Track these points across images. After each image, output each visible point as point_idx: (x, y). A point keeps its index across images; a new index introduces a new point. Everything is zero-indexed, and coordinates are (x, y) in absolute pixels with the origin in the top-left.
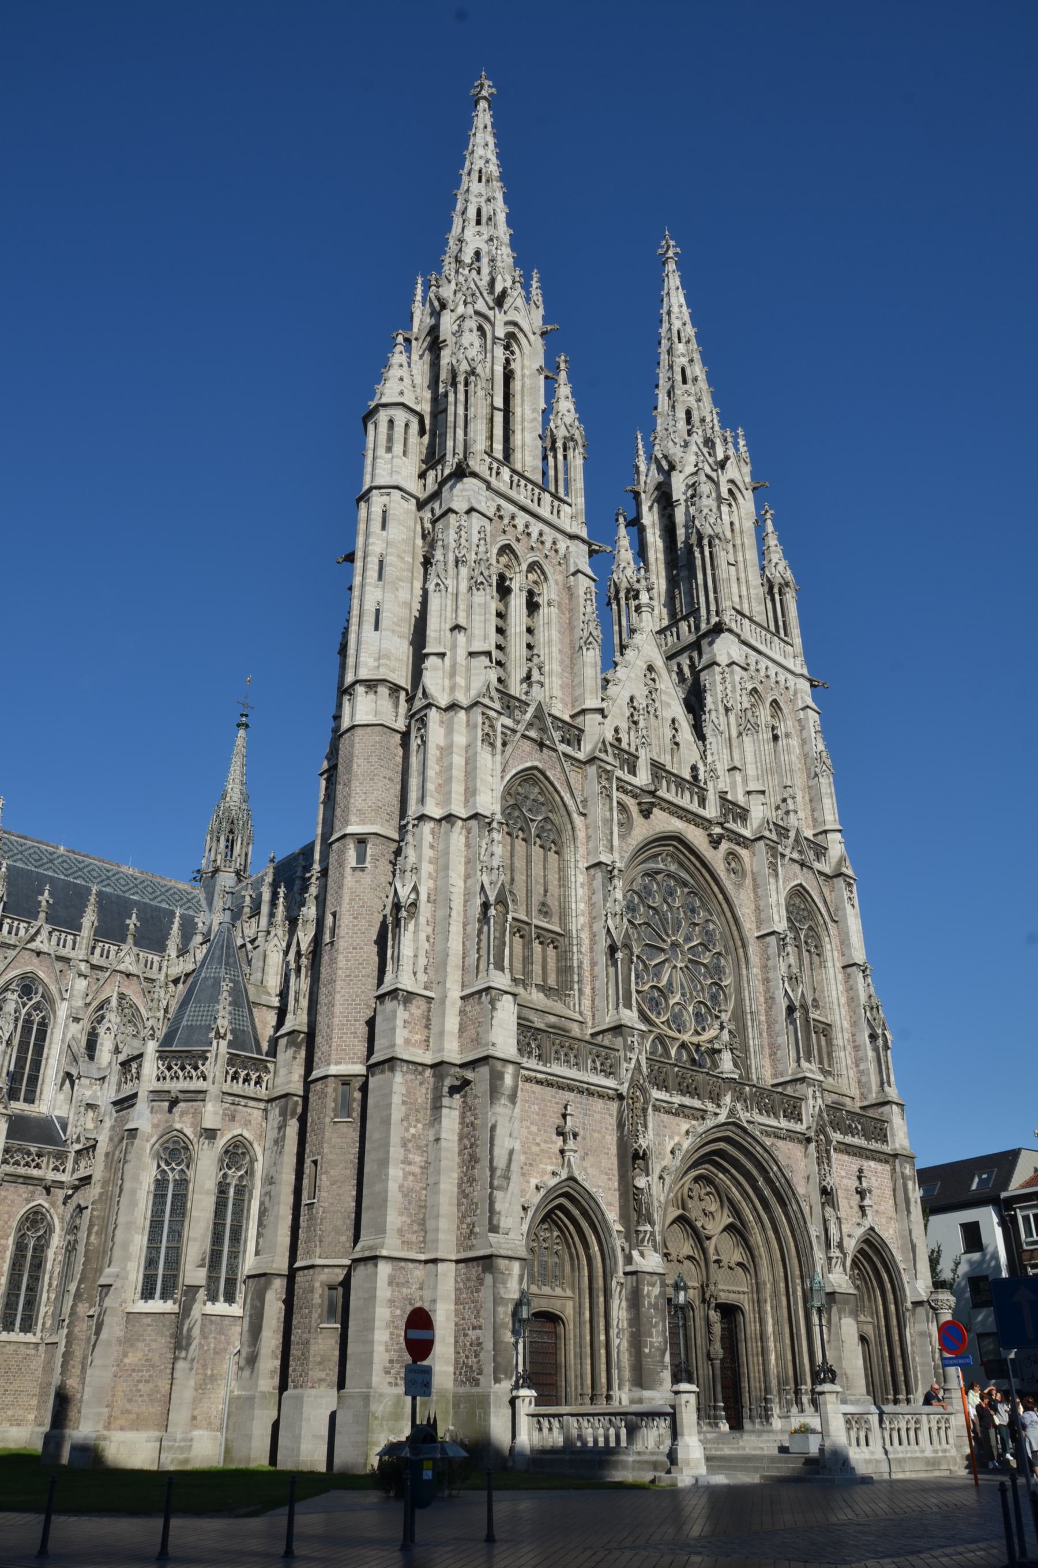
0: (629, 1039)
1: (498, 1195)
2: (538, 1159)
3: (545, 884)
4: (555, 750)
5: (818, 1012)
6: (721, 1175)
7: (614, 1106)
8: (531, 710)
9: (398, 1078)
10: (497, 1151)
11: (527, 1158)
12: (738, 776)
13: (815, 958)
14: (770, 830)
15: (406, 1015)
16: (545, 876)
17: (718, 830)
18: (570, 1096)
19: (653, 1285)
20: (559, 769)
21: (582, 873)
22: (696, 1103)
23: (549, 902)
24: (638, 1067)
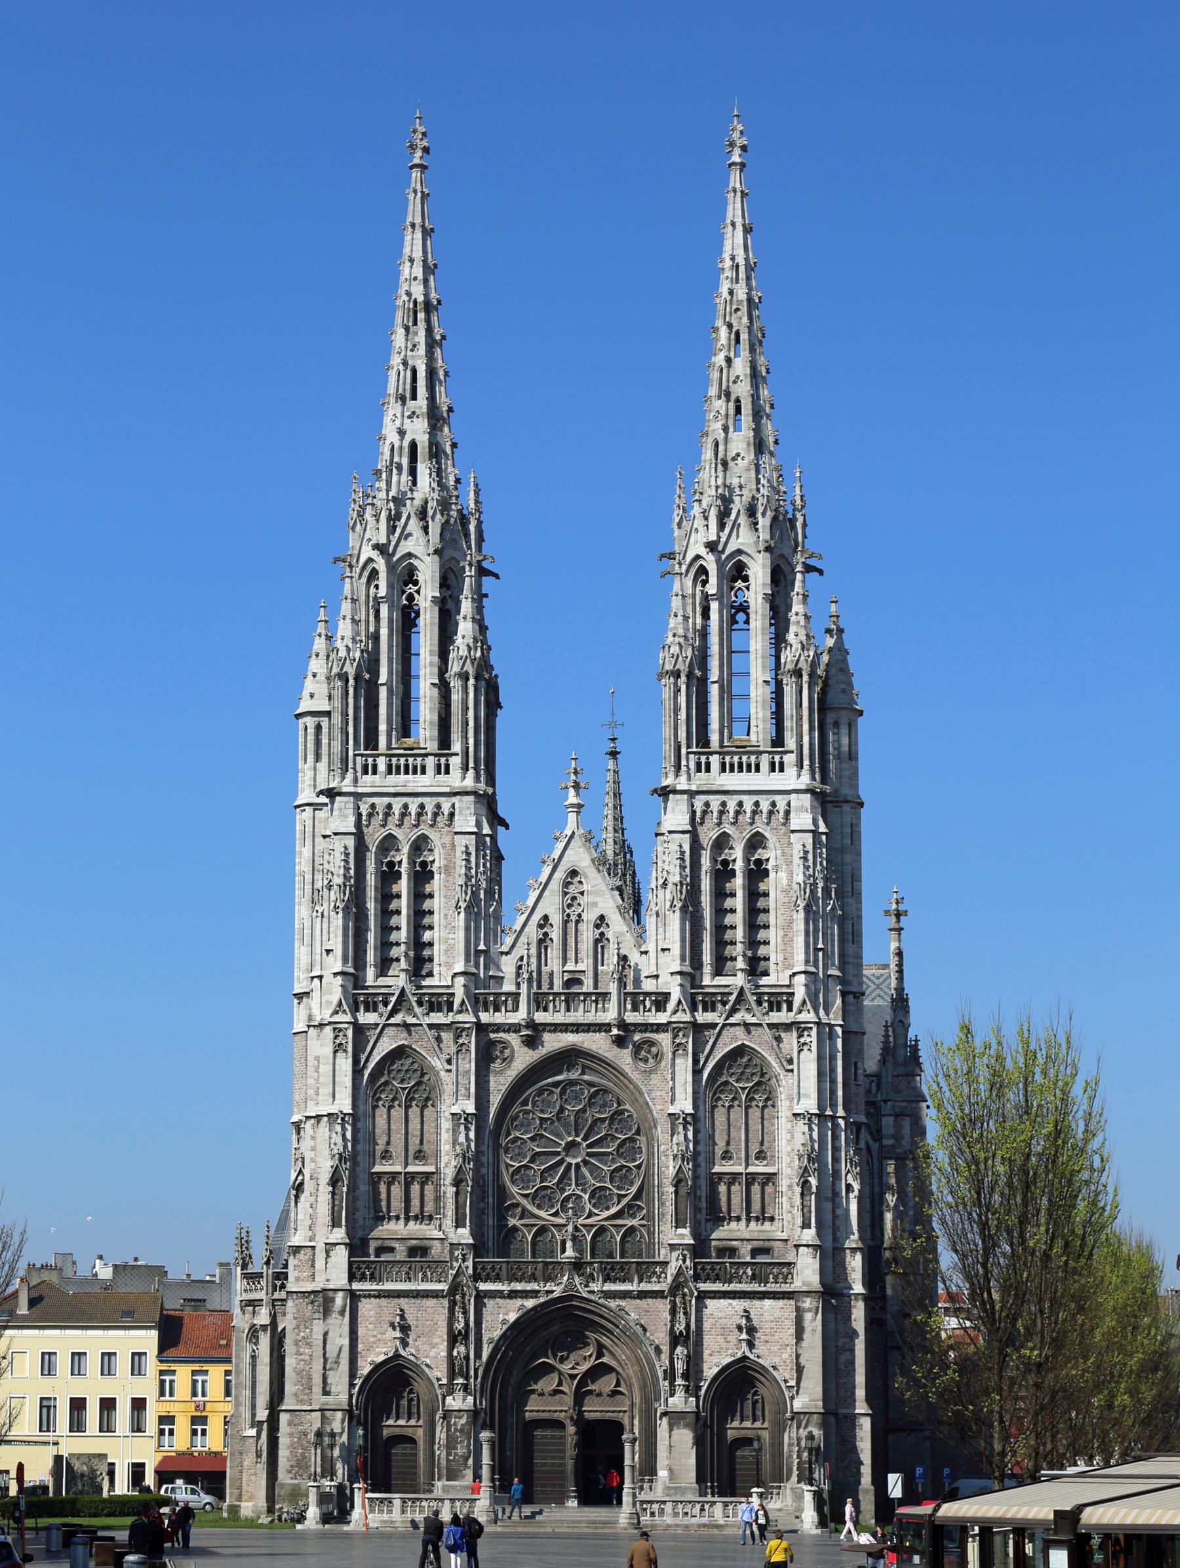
0: (456, 1253)
8: (393, 999)
9: (290, 1303)
10: (328, 1347)
15: (296, 1262)
17: (615, 1031)
18: (403, 1302)
19: (460, 1418)
21: (447, 1120)
22: (533, 1286)
23: (425, 1147)
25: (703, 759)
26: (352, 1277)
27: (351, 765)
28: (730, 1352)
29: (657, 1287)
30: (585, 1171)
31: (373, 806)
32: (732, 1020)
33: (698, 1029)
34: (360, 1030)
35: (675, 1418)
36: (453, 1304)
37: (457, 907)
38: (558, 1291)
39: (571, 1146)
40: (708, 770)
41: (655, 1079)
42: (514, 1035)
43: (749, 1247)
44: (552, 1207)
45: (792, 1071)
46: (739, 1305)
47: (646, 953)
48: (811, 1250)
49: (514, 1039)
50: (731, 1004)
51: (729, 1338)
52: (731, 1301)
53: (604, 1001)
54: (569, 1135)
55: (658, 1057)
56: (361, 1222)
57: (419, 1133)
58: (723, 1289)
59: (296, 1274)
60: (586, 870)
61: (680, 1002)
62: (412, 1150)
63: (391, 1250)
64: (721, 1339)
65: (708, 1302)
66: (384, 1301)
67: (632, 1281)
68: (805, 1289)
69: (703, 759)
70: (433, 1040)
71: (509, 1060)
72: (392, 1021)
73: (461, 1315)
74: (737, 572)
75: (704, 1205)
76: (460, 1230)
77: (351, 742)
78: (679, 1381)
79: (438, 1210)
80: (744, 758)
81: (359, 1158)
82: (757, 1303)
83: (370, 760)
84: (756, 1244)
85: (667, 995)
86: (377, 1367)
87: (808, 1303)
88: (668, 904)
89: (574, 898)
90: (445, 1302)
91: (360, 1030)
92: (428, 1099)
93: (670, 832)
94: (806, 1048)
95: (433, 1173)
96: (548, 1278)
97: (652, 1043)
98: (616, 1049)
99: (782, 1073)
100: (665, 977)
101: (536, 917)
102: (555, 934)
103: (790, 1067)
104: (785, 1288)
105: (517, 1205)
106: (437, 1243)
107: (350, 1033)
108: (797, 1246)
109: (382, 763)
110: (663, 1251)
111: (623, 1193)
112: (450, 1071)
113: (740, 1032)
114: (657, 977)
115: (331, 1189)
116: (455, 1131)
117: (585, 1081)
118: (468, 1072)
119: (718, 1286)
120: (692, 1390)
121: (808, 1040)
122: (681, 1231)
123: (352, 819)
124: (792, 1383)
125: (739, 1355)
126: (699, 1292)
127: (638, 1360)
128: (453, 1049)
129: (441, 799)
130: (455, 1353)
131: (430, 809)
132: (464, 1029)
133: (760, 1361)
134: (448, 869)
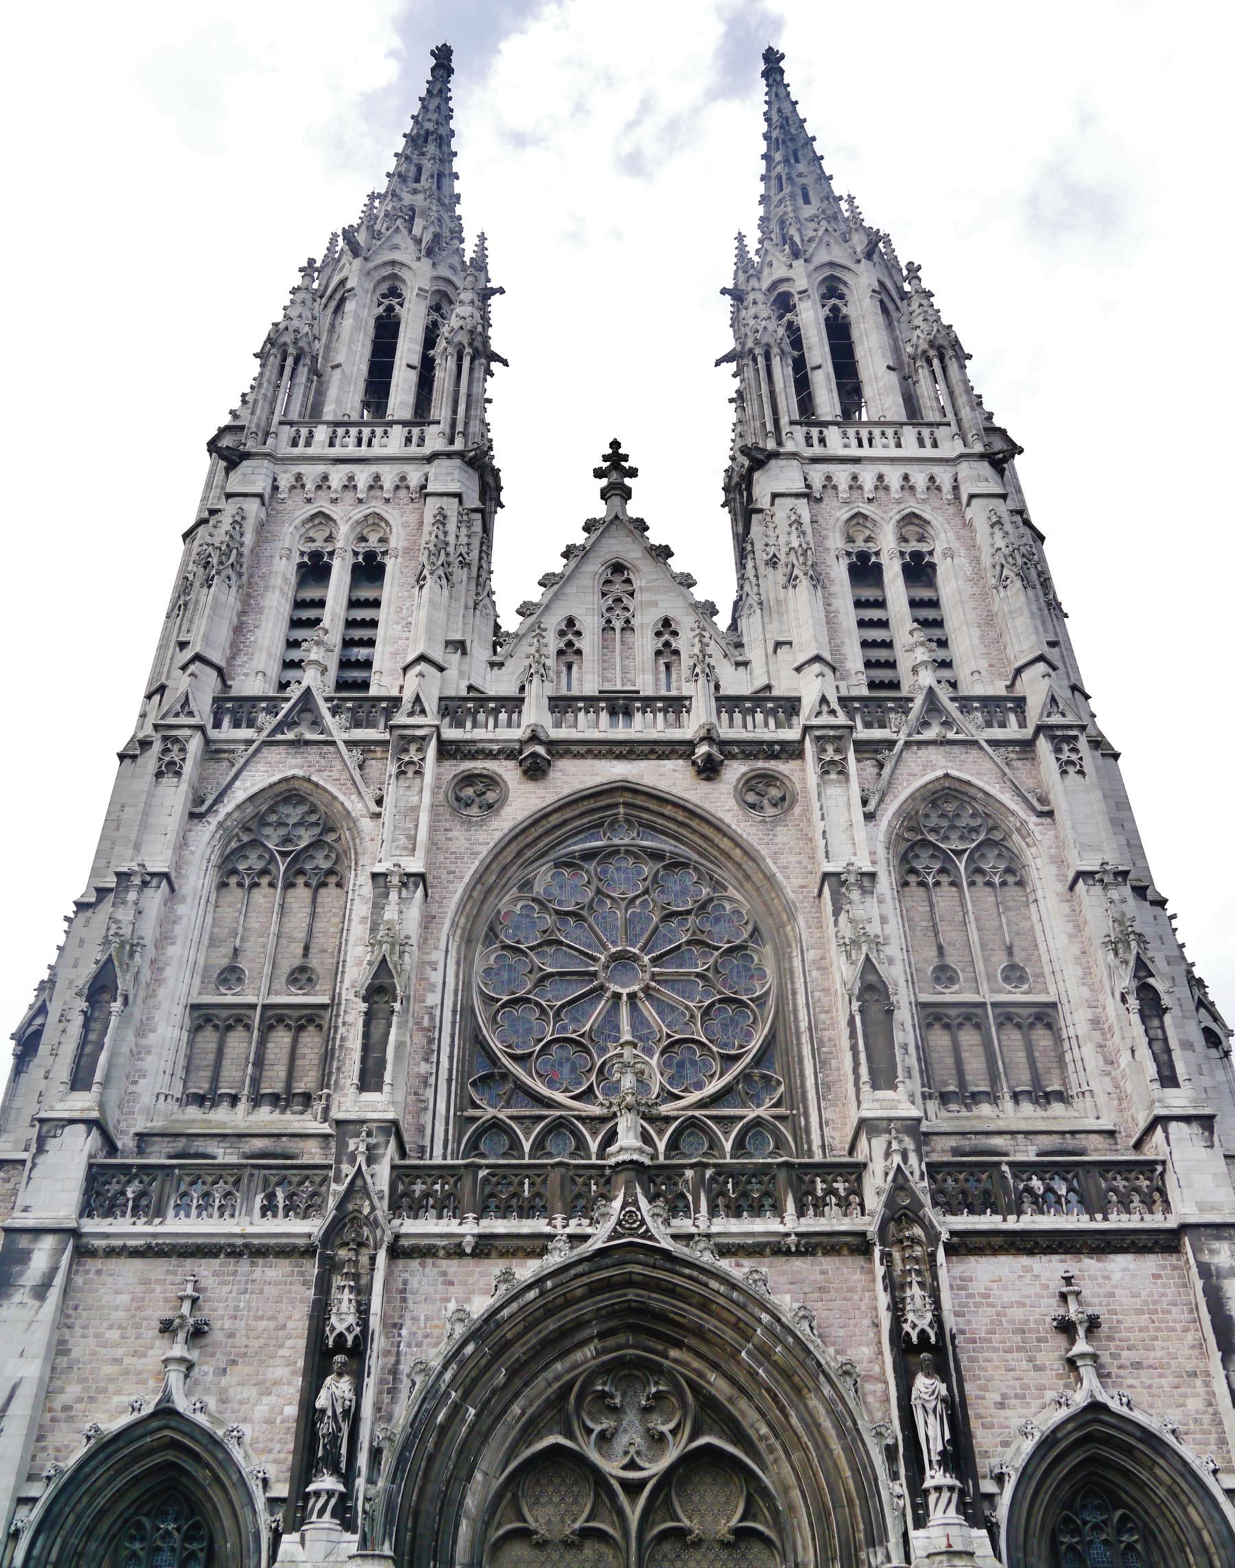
0: (352, 1144)
2: (111, 1388)
4: (333, 743)
5: (1025, 987)
6: (673, 1353)
8: (286, 706)
11: (86, 1389)
16: (311, 927)
18: (206, 1269)
20: (338, 765)
22: (538, 1225)
23: (314, 961)
24: (357, 1188)
26: (87, 1210)
28: (1050, 1395)
29: (845, 1225)
30: (648, 1009)
31: (299, 477)
32: (917, 737)
33: (860, 746)
36: (330, 1267)
37: (421, 579)
38: (600, 1235)
39: (622, 960)
41: (784, 835)
42: (511, 764)
45: (1050, 814)
46: (1051, 1268)
47: (745, 664)
48: (1195, 1128)
51: (1041, 1358)
52: (1025, 1260)
53: (678, 713)
54: (614, 943)
55: (784, 802)
56: (146, 1099)
57: (302, 935)
58: (1004, 1226)
60: (638, 563)
61: (824, 700)
62: (286, 966)
64: (1018, 1360)
66: (157, 1269)
67: (778, 1210)
69: (815, 432)
70: (352, 765)
72: (279, 737)
73: (346, 1295)
74: (832, 289)
75: (913, 1061)
78: (935, 1477)
79: (324, 1082)
81: (169, 972)
82: (1089, 1264)
86: (106, 1449)
90: (313, 1268)
91: (213, 752)
92: (331, 872)
93: (775, 496)
94: (1071, 769)
95: (324, 1007)
96: (581, 1205)
97: (769, 779)
98: (704, 786)
99: (1032, 820)
101: (553, 622)
102: (588, 643)
103: (1046, 809)
104: (1156, 1221)
105: (506, 1075)
109: (321, 433)
111: (733, 1052)
112: (378, 815)
116: (378, 907)
117: (644, 849)
118: (416, 809)
119: (987, 1221)
120: (974, 1509)
121: (1074, 757)
122: (888, 1094)
125: (1080, 1399)
126: (953, 1233)
127: (812, 1425)
128: (392, 768)
130: (322, 1402)
131: (388, 481)
132: (414, 739)
133: (1138, 1416)
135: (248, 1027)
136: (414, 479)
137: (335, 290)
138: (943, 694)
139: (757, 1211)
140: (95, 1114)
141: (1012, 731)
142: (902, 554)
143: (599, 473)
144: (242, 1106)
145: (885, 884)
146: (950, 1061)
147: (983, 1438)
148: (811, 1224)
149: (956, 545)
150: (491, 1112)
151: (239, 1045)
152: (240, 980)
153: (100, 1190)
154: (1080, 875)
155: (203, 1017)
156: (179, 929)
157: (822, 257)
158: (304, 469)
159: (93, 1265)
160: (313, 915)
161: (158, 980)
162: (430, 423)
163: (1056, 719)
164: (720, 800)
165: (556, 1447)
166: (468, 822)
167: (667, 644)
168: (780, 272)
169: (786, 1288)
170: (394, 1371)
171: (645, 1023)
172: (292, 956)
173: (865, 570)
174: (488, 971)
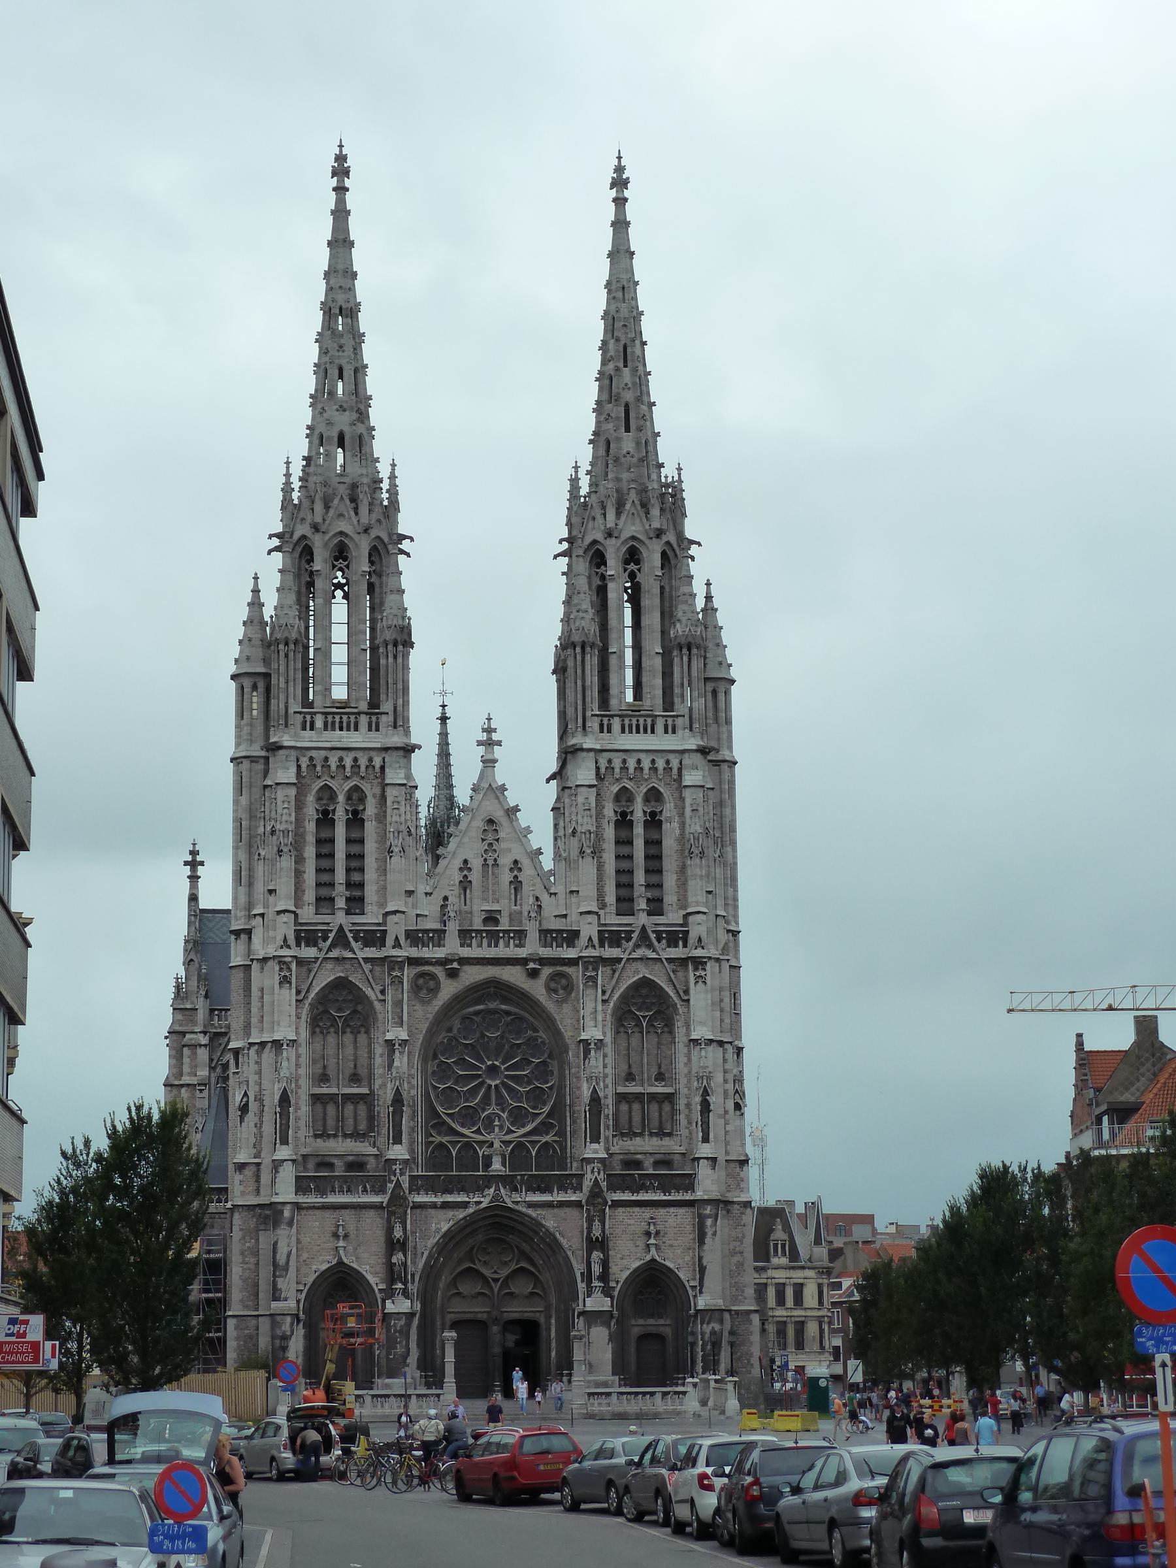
1: (279, 1280)
3: (355, 1061)
7: (380, 1211)
8: (331, 935)
9: (236, 1216)
10: (278, 1256)
12: (574, 899)
13: (666, 1037)
14: (594, 947)
16: (355, 1055)
22: (462, 1198)
25: (605, 721)
27: (291, 722)
32: (634, 955)
34: (300, 962)
35: (592, 1317)
36: (391, 1213)
40: (609, 731)
41: (567, 1008)
42: (440, 968)
43: (652, 1160)
44: (474, 1125)
45: (688, 1001)
46: (647, 1213)
49: (439, 971)
50: (633, 940)
51: (638, 1243)
55: (569, 988)
58: (633, 1198)
59: (241, 1188)
61: (590, 939)
63: (331, 1166)
65: (621, 1210)
66: (328, 1214)
67: (551, 1192)
68: (706, 1197)
71: (435, 990)
72: (331, 955)
74: (633, 556)
76: (397, 1147)
77: (291, 701)
78: (596, 1283)
80: (641, 721)
82: (662, 1211)
83: (308, 718)
84: (658, 1157)
85: (576, 934)
87: (708, 1210)
88: (577, 852)
89: (490, 845)
93: (577, 786)
94: (700, 980)
96: (480, 1189)
100: (574, 917)
102: (475, 876)
105: (445, 1122)
106: (372, 1160)
107: (294, 966)
108: (699, 1159)
109: (319, 724)
110: (575, 1165)
113: (639, 965)
114: (565, 916)
115: (278, 1109)
119: (627, 1196)
120: (607, 1292)
122: (595, 1146)
123: (294, 770)
124: (696, 1283)
125: (648, 1258)
128: (388, 981)
129: (372, 754)
130: (394, 1260)
133: (667, 1263)
134: (381, 818)
135: (336, 1103)
136: (377, 762)
137: (300, 539)
138: (649, 931)
139: (543, 1191)
140: (294, 1157)
141: (678, 952)
142: (645, 812)
143: (480, 743)
144: (340, 1139)
145: (608, 1039)
146: (627, 1117)
147: (614, 1269)
148: (562, 1197)
149: (674, 812)
150: (439, 1139)
151: (331, 1110)
152: (328, 1080)
153: (302, 1185)
154: (691, 1040)
155: (316, 1098)
156: (302, 1060)
157: (626, 534)
158: (314, 754)
159: (304, 1212)
160: (356, 1048)
161: (298, 1087)
162: (382, 713)
163: (699, 953)
164: (537, 989)
165: (470, 1268)
166: (424, 1002)
167: (516, 877)
168: (599, 536)
169: (550, 1221)
170: (415, 1248)
171: (502, 1097)
172: (349, 1070)
173: (624, 822)
174: (434, 1073)
